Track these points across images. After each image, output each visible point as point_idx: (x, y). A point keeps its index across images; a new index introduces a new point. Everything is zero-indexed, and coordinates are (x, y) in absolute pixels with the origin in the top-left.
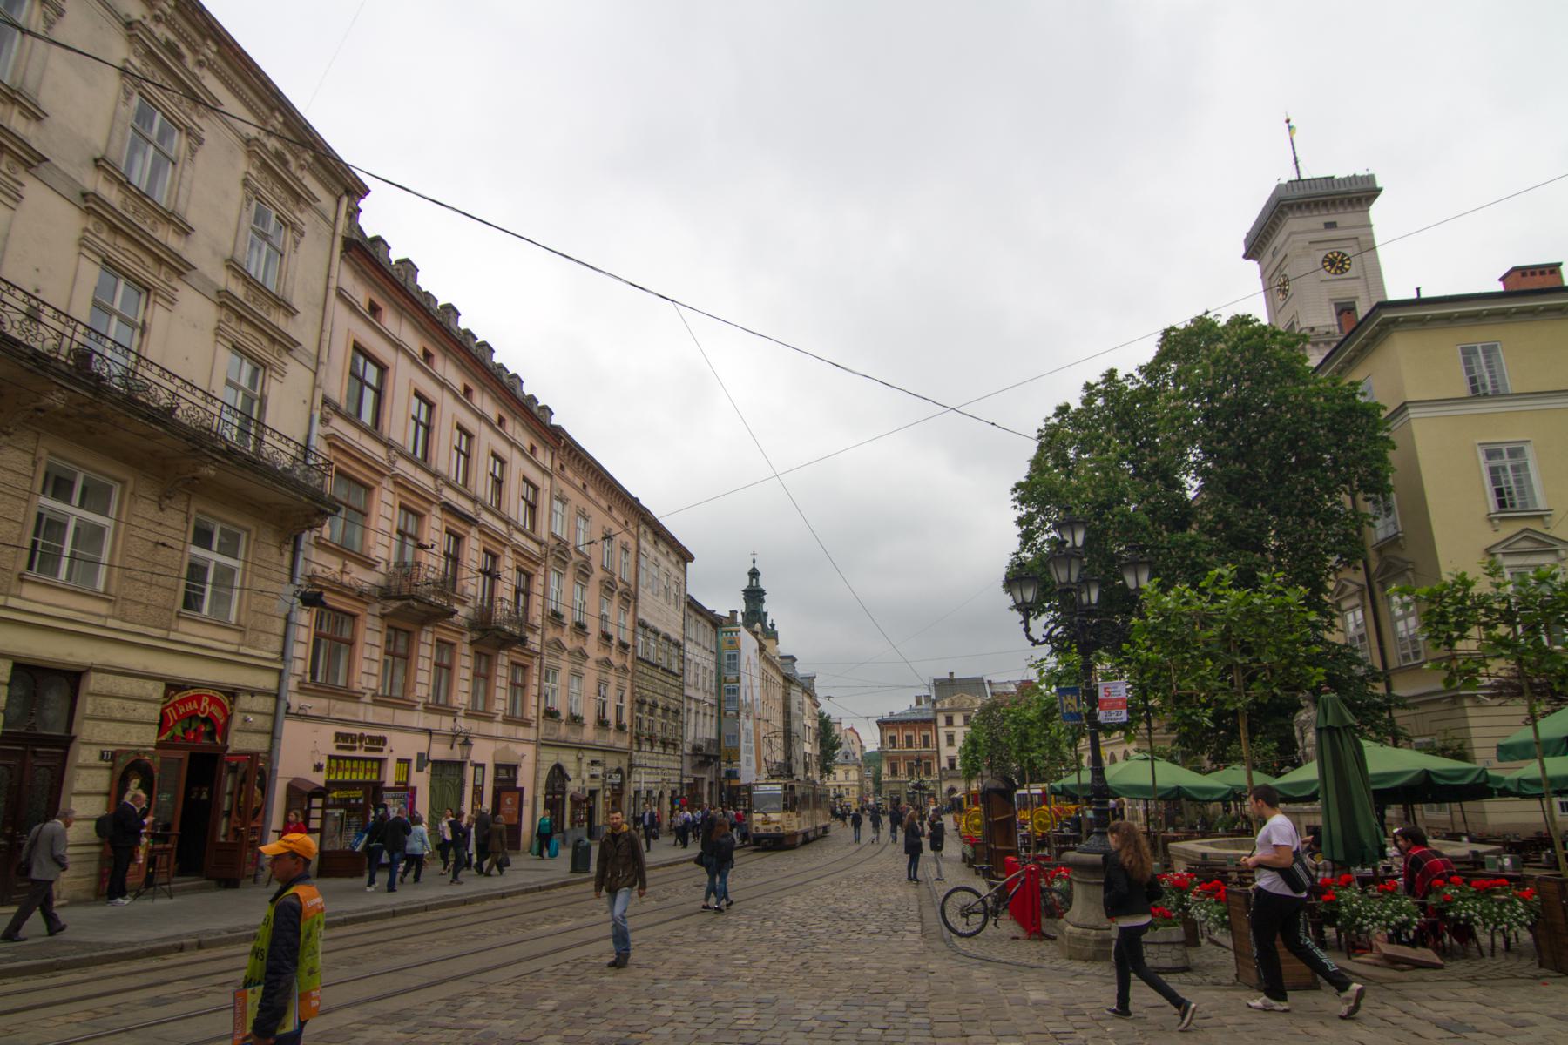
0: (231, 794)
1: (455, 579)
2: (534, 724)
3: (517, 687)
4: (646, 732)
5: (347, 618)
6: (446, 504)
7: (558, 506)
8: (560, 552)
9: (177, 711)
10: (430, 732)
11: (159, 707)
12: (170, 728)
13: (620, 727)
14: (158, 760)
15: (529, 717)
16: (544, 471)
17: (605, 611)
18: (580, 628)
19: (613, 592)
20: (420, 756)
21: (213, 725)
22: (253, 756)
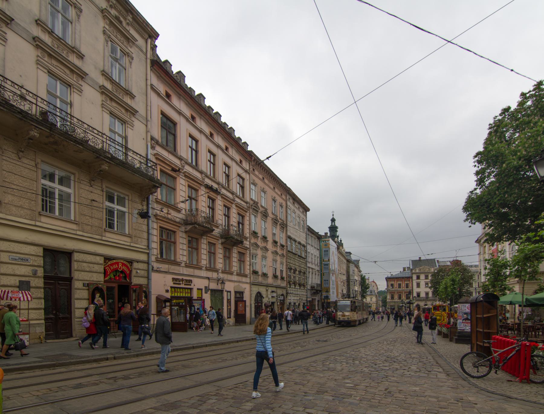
1: (213, 216)
2: (249, 276)
3: (241, 261)
4: (293, 281)
7: (253, 187)
8: (255, 207)
9: (110, 269)
10: (209, 278)
11: (103, 267)
12: (109, 275)
13: (282, 278)
14: (105, 287)
15: (247, 273)
16: (246, 171)
17: (274, 232)
18: (265, 238)
19: (277, 224)
20: (206, 287)
21: (125, 274)
22: (141, 286)
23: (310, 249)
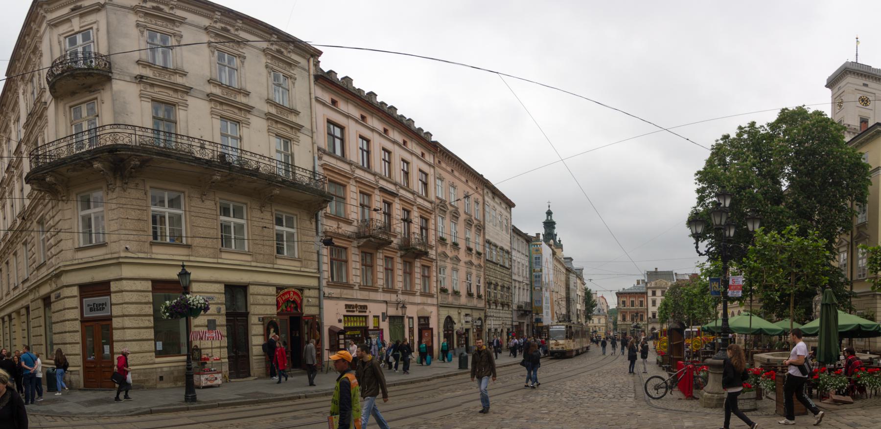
0: (307, 334)
1: (390, 225)
3: (426, 278)
4: (493, 299)
5: (343, 250)
6: (381, 188)
7: (439, 182)
8: (442, 206)
9: (282, 299)
10: (386, 302)
11: (275, 298)
14: (278, 320)
15: (433, 292)
16: (430, 165)
17: (468, 236)
18: (455, 245)
19: (471, 225)
20: (383, 314)
21: (296, 304)
22: (314, 317)
23: (515, 255)
